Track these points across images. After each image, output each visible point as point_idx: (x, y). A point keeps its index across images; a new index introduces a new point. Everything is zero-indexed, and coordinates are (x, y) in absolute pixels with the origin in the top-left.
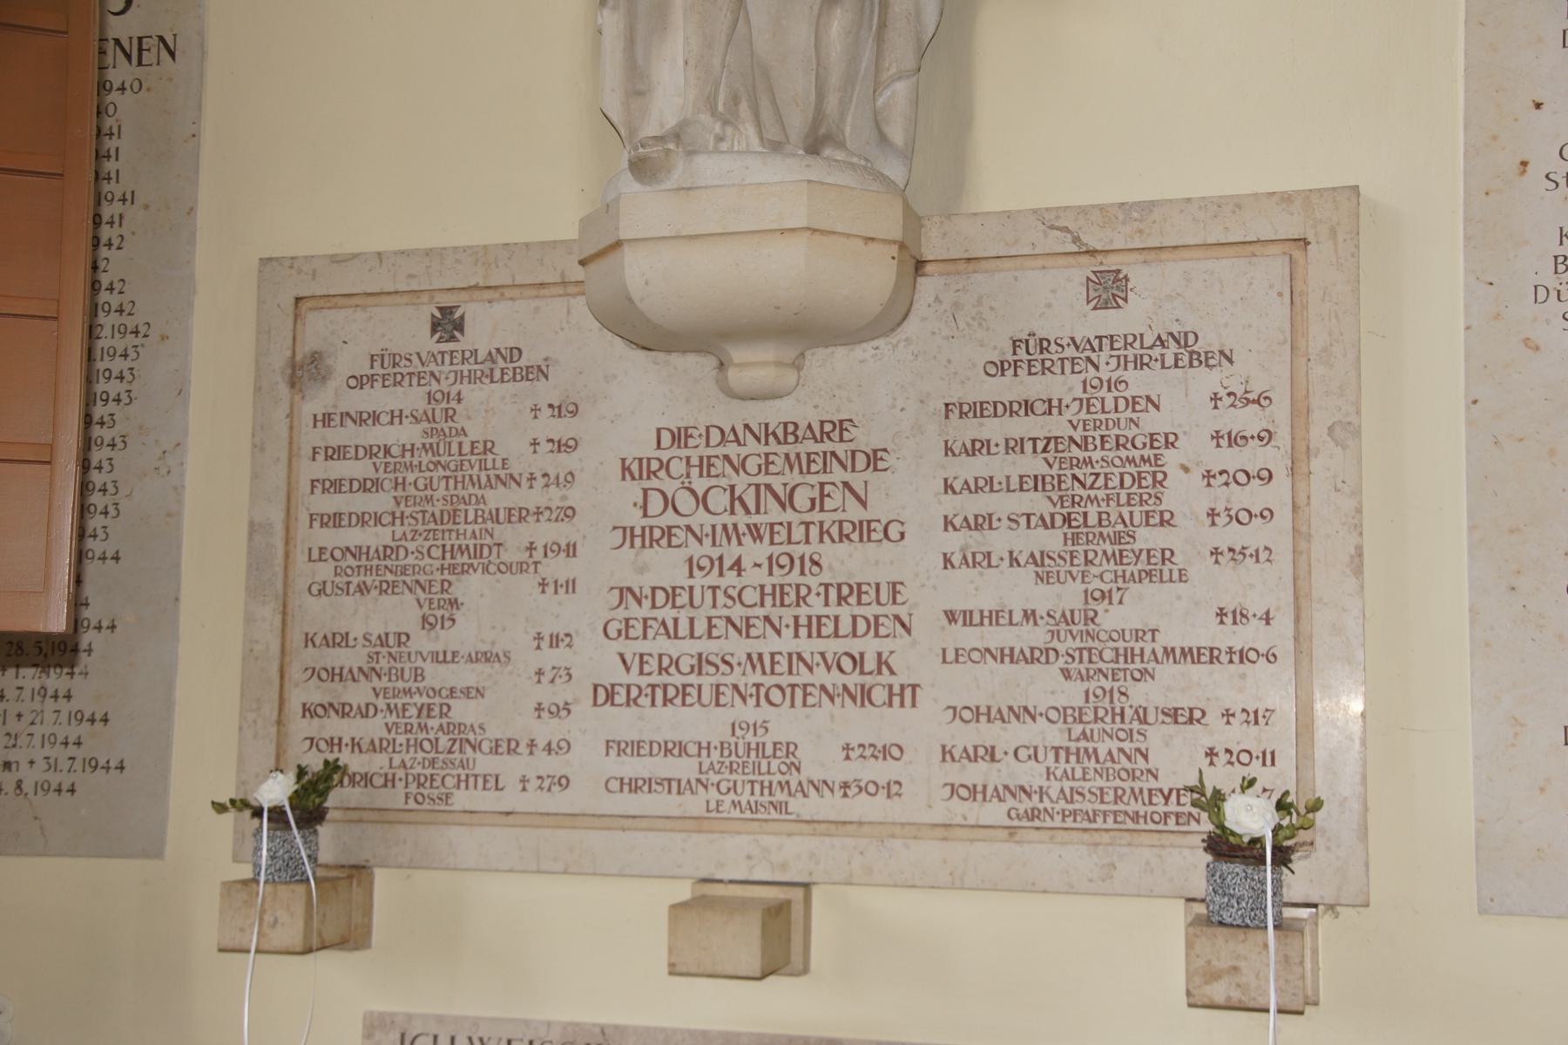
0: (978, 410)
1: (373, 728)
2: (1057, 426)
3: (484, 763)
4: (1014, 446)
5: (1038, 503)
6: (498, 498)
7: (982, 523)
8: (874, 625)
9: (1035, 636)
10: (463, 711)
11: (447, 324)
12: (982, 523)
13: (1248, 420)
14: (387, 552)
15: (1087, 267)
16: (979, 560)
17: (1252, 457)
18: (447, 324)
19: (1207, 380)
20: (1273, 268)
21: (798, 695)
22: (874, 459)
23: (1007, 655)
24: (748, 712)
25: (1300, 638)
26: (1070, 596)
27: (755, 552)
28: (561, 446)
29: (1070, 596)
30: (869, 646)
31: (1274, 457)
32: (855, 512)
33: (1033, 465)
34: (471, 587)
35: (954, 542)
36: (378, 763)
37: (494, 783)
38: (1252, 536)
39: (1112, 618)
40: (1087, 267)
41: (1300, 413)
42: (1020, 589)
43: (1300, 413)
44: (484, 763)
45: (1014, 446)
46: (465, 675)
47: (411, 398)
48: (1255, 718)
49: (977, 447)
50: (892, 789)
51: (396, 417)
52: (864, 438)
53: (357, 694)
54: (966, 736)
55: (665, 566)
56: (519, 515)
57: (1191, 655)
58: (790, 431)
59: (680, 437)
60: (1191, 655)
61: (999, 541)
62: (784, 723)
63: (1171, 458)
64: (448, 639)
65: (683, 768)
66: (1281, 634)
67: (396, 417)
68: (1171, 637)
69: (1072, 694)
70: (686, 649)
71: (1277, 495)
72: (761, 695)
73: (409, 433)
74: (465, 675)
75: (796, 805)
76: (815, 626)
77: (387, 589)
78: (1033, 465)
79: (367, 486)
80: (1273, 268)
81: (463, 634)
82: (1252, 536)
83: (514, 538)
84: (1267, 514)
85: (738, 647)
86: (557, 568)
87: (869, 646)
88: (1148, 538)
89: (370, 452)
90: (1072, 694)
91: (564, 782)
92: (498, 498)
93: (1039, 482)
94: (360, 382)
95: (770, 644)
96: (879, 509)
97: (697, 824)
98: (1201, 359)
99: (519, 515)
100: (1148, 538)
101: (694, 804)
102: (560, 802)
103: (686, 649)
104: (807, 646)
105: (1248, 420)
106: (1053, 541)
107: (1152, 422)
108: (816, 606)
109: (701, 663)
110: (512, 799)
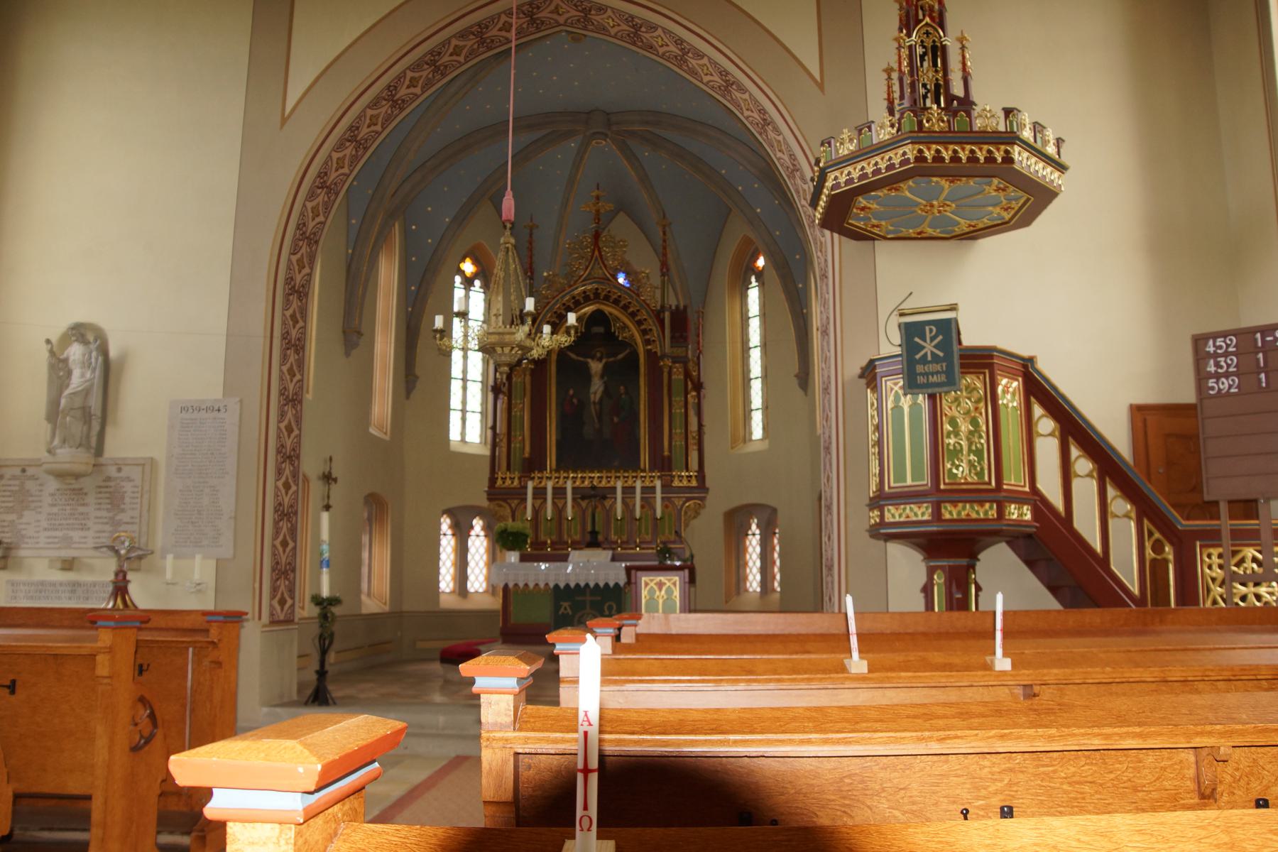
0: (100, 487)
1: (7, 535)
2: (111, 490)
3: (26, 540)
4: (106, 492)
5: (107, 501)
6: (31, 499)
7: (100, 504)
8: (84, 519)
9: (105, 520)
10: (24, 532)
11: (24, 471)
12: (100, 504)
13: (136, 490)
14: (12, 507)
15: (117, 466)
16: (99, 509)
17: (136, 495)
18: (24, 471)
19: (131, 484)
20: (140, 468)
21: (73, 529)
22: (86, 494)
23: (103, 523)
24: (65, 532)
25: (140, 521)
26: (111, 514)
27: (68, 508)
28: (41, 491)
29: (111, 514)
30: (83, 522)
31: (139, 495)
32: (82, 502)
33: (107, 495)
34: (26, 513)
35: (98, 506)
36: (9, 541)
37: (27, 543)
38: (134, 506)
39: (118, 518)
40: (117, 466)
41: (142, 489)
42: (104, 514)
43: (142, 489)
44: (26, 540)
45: (106, 492)
46: (23, 526)
47: (17, 482)
48: (134, 532)
49: (100, 493)
50: (85, 543)
51: (14, 485)
52: (85, 491)
53: (6, 529)
54: (98, 535)
55: (55, 510)
56: (33, 501)
57: (127, 523)
58: (74, 490)
59: (58, 490)
60: (127, 523)
61: (103, 506)
62: (71, 533)
63: (126, 495)
64: (21, 521)
65: (56, 540)
66: (138, 520)
67: (14, 485)
68: (125, 520)
69: (111, 529)
70: (57, 522)
71: (139, 500)
72: (68, 529)
73: (17, 488)
74: (23, 526)
75: (74, 546)
76: (76, 519)
77: (13, 513)
78: (107, 495)
79: (10, 496)
80: (140, 468)
81: (24, 520)
82: (134, 506)
83: (33, 505)
84: (137, 503)
85: (64, 522)
86: (39, 510)
87: (83, 522)
88: (122, 506)
89: (9, 491)
90: (111, 529)
91: (37, 543)
92: (31, 499)
93: (108, 498)
94: (10, 479)
95: (71, 521)
96: (85, 502)
97: (59, 548)
98: (131, 481)
99: (33, 501)
100: (122, 506)
101: (58, 546)
102: (37, 546)
103: (57, 522)
104: (74, 522)
105: (136, 490)
106: (109, 506)
107: (124, 490)
108: (76, 516)
109: (60, 525)
110: (30, 546)
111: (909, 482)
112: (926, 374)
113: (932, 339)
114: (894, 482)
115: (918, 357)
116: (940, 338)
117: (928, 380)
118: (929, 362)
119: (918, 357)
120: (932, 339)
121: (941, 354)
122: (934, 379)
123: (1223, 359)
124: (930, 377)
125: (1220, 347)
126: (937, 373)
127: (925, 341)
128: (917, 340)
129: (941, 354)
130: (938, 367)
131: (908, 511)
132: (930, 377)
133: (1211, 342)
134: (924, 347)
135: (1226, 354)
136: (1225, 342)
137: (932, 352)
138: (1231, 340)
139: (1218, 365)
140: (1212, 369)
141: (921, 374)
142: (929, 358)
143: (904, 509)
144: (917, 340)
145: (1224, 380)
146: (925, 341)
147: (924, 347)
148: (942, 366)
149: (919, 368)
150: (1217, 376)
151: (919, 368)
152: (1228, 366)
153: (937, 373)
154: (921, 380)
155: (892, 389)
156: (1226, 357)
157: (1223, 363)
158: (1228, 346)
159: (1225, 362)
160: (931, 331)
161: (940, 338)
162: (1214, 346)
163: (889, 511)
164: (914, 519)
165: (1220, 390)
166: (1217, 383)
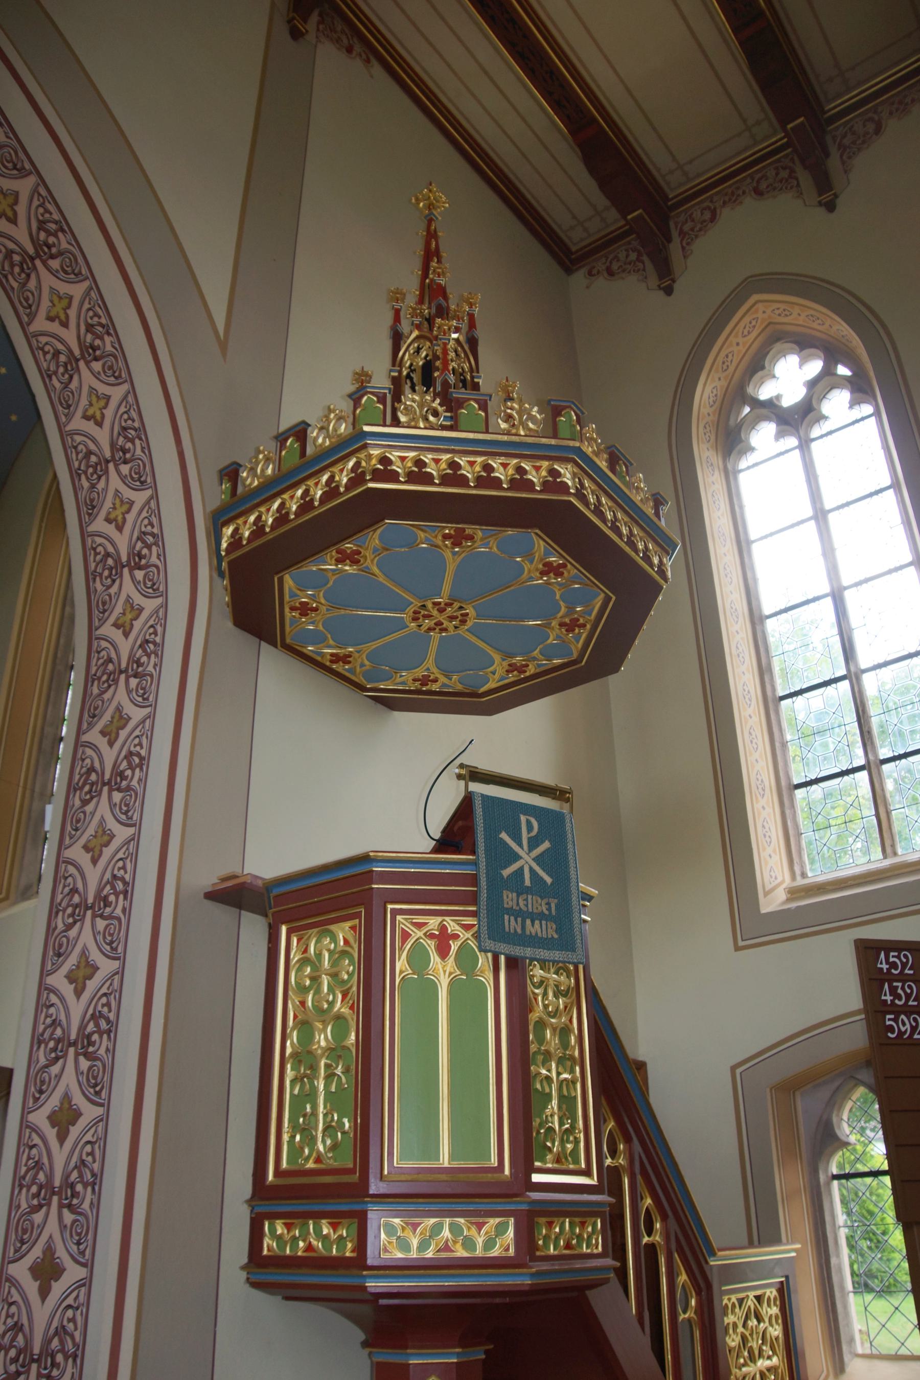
111: (445, 1159)
112: (518, 914)
113: (534, 843)
114: (401, 1158)
115: (506, 873)
116: (546, 845)
117: (523, 927)
118: (528, 891)
119: (506, 873)
120: (534, 843)
121: (549, 880)
122: (534, 928)
123: (900, 984)
124: (528, 922)
125: (894, 965)
126: (541, 916)
127: (518, 840)
128: (504, 836)
129: (549, 880)
130: (537, 904)
131: (446, 1233)
132: (528, 922)
133: (882, 955)
134: (517, 857)
135: (902, 978)
136: (898, 957)
137: (531, 870)
138: (905, 956)
139: (893, 991)
140: (889, 998)
141: (510, 911)
142: (527, 882)
143: (437, 1228)
144: (504, 836)
145: (903, 1017)
146: (518, 840)
147: (517, 857)
148: (548, 904)
149: (509, 899)
150: (897, 1012)
151: (509, 899)
152: (908, 996)
153: (541, 916)
154: (511, 924)
155: (406, 936)
156: (904, 982)
157: (900, 991)
158: (904, 965)
159: (903, 988)
160: (530, 827)
161: (546, 845)
162: (887, 962)
163: (390, 1230)
164: (461, 1252)
165: (901, 1034)
166: (895, 1020)
